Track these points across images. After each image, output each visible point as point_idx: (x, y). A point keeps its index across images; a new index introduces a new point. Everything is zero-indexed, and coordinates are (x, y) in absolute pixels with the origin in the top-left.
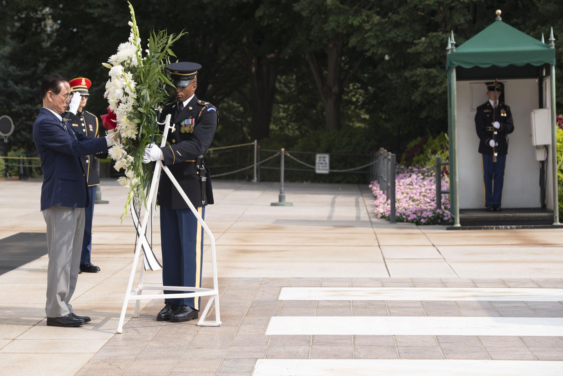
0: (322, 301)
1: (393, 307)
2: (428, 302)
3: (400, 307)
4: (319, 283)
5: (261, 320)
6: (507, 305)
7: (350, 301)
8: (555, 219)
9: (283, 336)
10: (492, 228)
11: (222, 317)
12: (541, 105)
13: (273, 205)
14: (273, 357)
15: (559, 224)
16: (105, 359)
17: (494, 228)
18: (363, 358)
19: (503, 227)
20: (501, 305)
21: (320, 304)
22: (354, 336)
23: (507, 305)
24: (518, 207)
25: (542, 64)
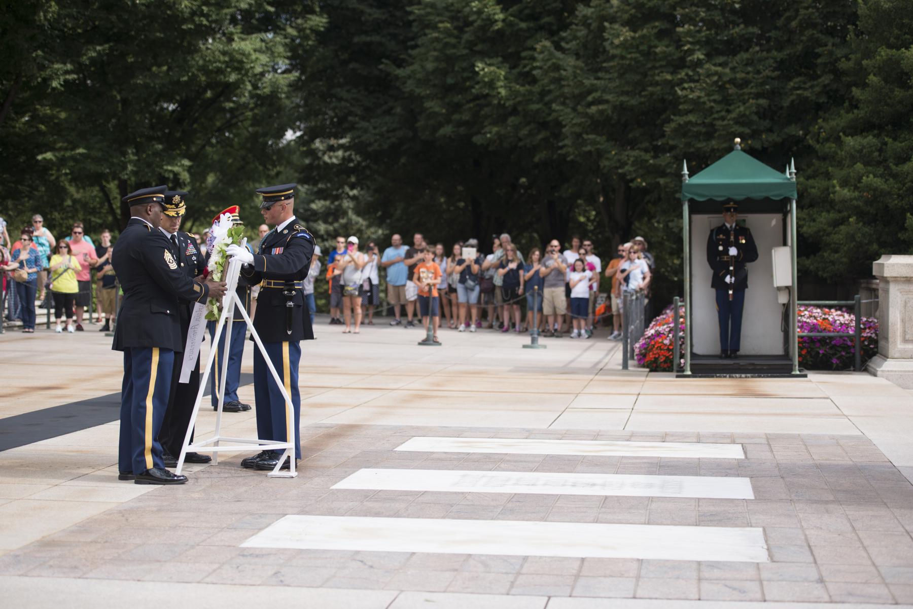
3: (516, 462)
4: (458, 433)
5: (346, 472)
7: (468, 454)
8: (794, 367)
10: (725, 377)
12: (785, 244)
15: (798, 373)
16: (125, 510)
17: (728, 376)
18: (404, 517)
19: (737, 375)
24: (758, 354)
25: (782, 197)
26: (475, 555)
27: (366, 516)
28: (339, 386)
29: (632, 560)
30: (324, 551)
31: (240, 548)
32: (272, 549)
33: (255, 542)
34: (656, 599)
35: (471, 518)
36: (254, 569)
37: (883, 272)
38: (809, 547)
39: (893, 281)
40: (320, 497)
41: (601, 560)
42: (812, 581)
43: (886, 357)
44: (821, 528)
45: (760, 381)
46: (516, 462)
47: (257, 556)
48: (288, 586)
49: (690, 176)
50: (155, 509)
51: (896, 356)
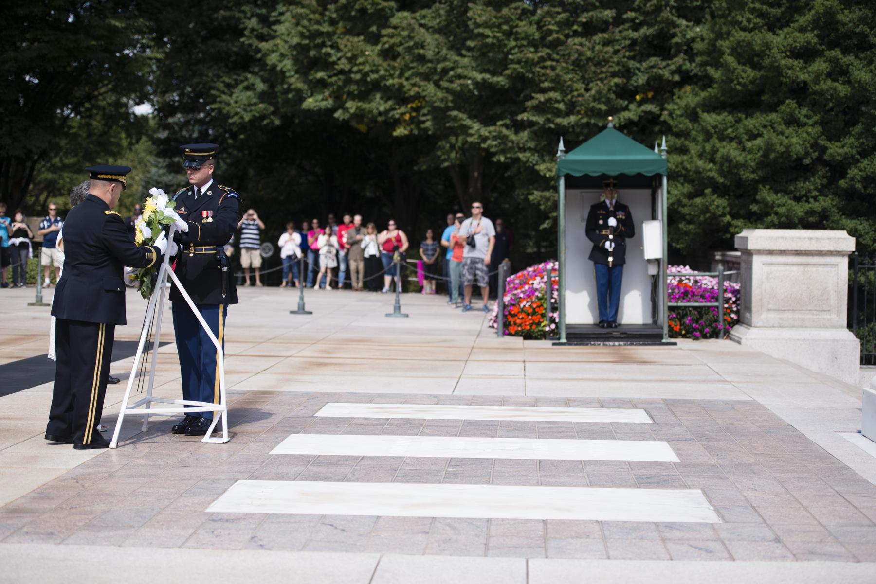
0: (358, 418)
3: (437, 427)
4: (369, 399)
5: (277, 437)
6: (552, 426)
7: (388, 419)
10: (599, 345)
12: (654, 218)
13: (387, 315)
14: (257, 478)
18: (353, 481)
19: (611, 343)
23: (552, 426)
26: (439, 518)
27: (317, 480)
28: (233, 353)
29: (592, 522)
30: (291, 515)
31: (208, 513)
32: (239, 513)
35: (419, 482)
36: (229, 534)
37: (747, 245)
39: (756, 254)
40: (263, 462)
41: (562, 522)
42: (771, 541)
43: (749, 325)
44: (756, 490)
46: (437, 427)
47: (227, 521)
48: (269, 549)
49: (567, 151)
50: (106, 475)
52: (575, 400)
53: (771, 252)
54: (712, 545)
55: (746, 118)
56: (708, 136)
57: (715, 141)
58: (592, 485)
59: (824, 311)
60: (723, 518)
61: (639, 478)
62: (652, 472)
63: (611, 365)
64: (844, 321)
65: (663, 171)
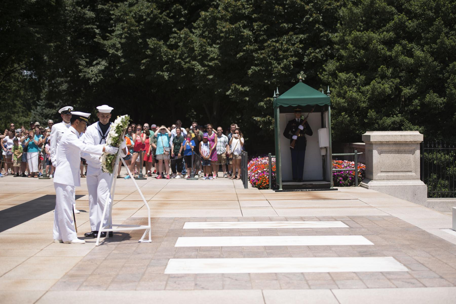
0: (206, 229)
1: (243, 232)
2: (262, 229)
3: (247, 232)
4: (205, 220)
5: (173, 239)
7: (221, 229)
9: (184, 247)
10: (299, 191)
11: (152, 238)
12: (323, 126)
14: (178, 258)
18: (225, 258)
20: (299, 230)
21: (205, 231)
22: (222, 247)
23: (302, 230)
30: (207, 274)
31: (166, 275)
32: (182, 274)
33: (169, 270)
34: (378, 288)
38: (422, 264)
40: (176, 250)
41: (336, 273)
43: (371, 179)
45: (315, 193)
46: (247, 232)
47: (178, 277)
50: (104, 259)
51: (376, 179)
52: (305, 218)
53: (381, 144)
54: (413, 281)
55: (361, 75)
56: (341, 85)
57: (345, 87)
58: (340, 256)
59: (409, 171)
60: (410, 269)
61: (360, 252)
62: (365, 249)
63: (311, 201)
64: (419, 176)
65: (328, 103)
